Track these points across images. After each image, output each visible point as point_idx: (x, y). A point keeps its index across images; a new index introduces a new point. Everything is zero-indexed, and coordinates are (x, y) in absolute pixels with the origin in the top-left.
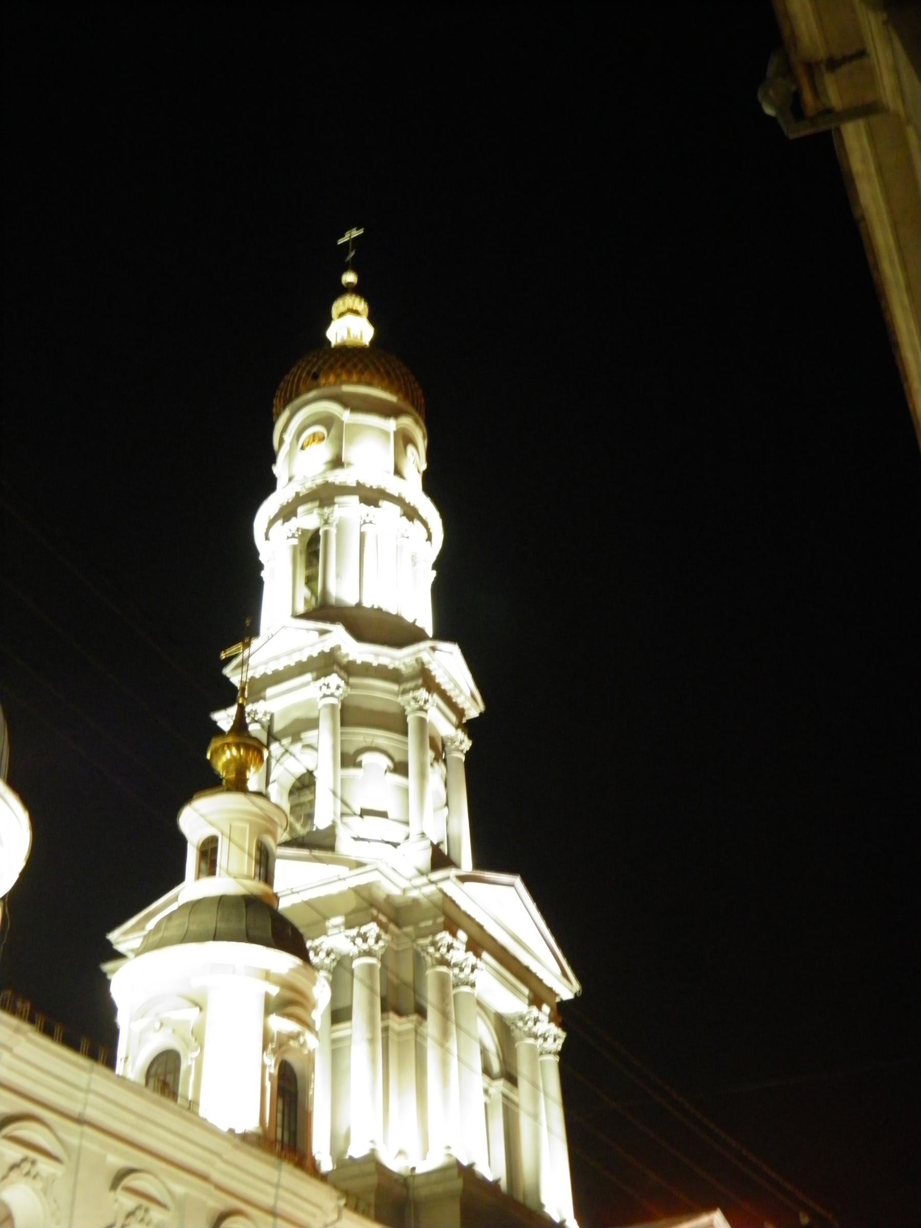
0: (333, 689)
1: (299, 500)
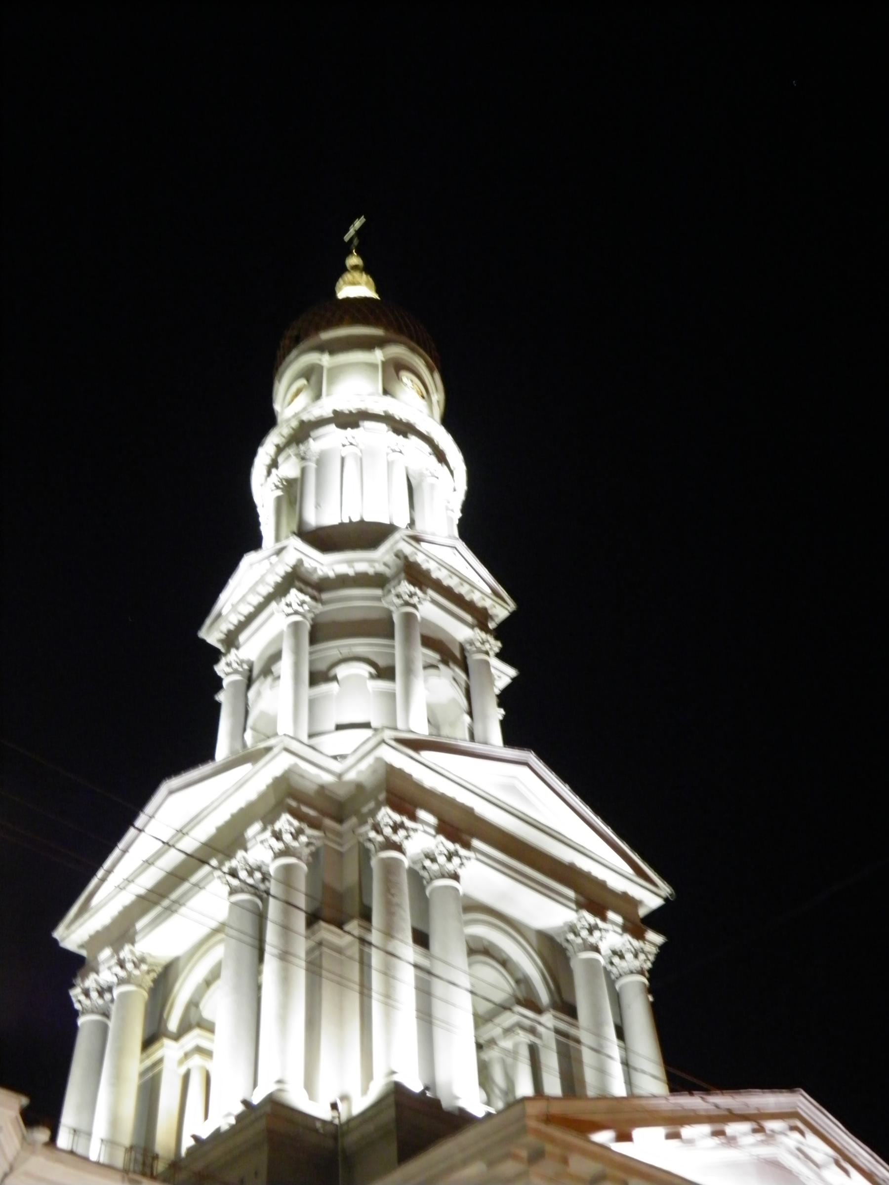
1: (280, 449)
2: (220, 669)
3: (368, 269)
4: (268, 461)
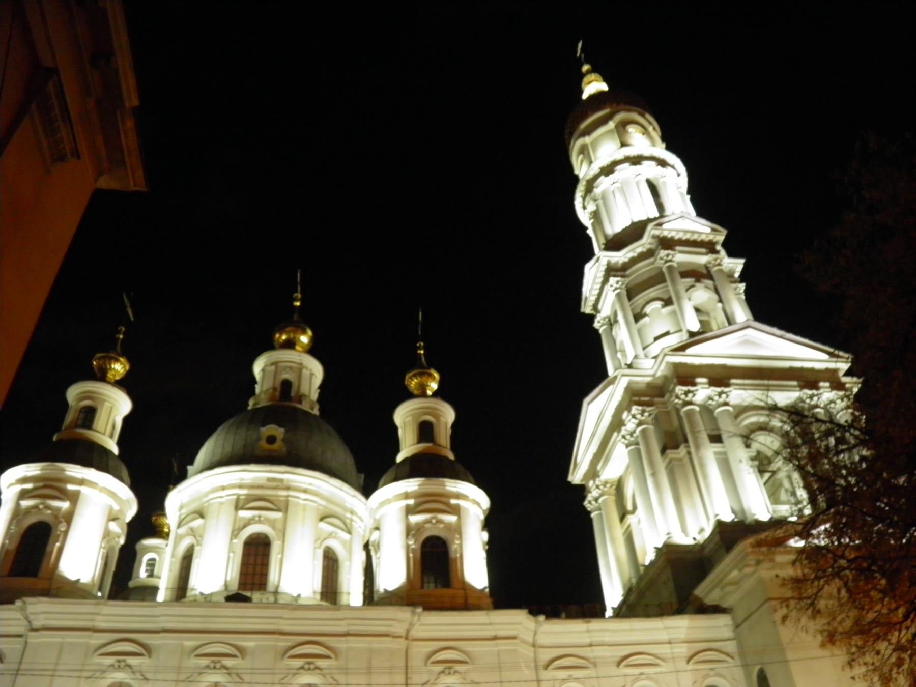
0: (615, 285)
1: (584, 198)
2: (596, 325)
3: (594, 70)
4: (581, 205)
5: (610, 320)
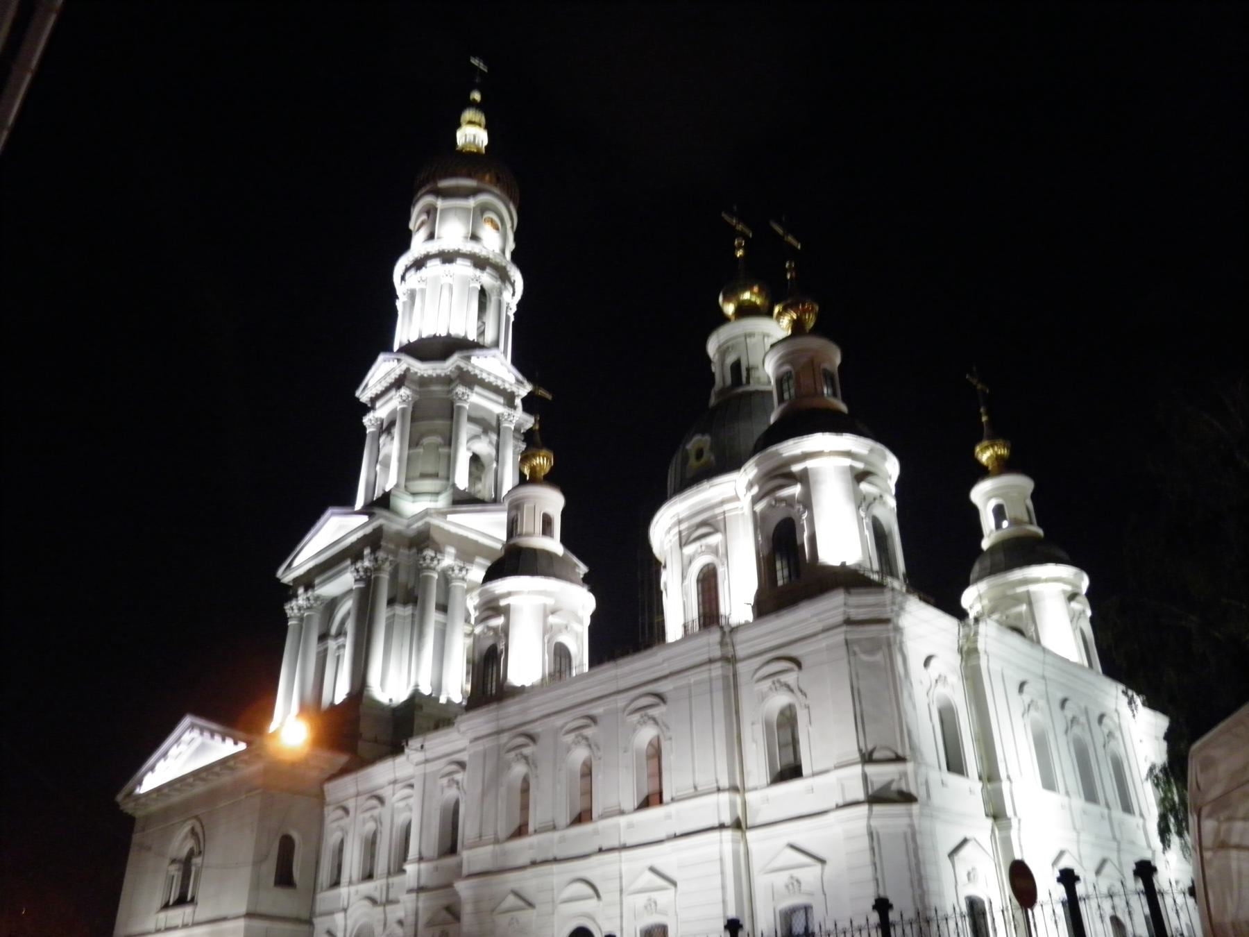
1: (407, 269)
5: (382, 424)
